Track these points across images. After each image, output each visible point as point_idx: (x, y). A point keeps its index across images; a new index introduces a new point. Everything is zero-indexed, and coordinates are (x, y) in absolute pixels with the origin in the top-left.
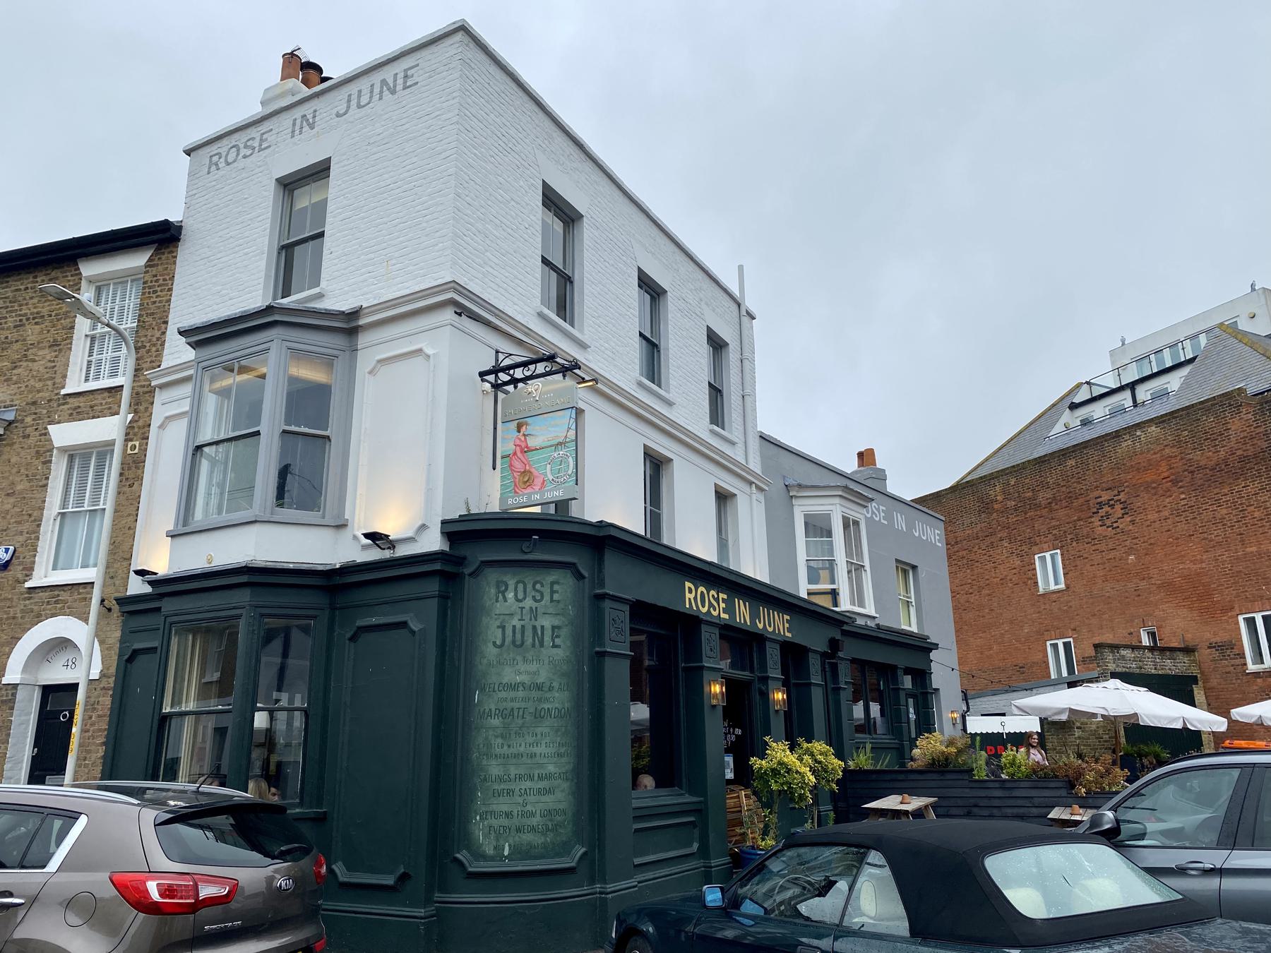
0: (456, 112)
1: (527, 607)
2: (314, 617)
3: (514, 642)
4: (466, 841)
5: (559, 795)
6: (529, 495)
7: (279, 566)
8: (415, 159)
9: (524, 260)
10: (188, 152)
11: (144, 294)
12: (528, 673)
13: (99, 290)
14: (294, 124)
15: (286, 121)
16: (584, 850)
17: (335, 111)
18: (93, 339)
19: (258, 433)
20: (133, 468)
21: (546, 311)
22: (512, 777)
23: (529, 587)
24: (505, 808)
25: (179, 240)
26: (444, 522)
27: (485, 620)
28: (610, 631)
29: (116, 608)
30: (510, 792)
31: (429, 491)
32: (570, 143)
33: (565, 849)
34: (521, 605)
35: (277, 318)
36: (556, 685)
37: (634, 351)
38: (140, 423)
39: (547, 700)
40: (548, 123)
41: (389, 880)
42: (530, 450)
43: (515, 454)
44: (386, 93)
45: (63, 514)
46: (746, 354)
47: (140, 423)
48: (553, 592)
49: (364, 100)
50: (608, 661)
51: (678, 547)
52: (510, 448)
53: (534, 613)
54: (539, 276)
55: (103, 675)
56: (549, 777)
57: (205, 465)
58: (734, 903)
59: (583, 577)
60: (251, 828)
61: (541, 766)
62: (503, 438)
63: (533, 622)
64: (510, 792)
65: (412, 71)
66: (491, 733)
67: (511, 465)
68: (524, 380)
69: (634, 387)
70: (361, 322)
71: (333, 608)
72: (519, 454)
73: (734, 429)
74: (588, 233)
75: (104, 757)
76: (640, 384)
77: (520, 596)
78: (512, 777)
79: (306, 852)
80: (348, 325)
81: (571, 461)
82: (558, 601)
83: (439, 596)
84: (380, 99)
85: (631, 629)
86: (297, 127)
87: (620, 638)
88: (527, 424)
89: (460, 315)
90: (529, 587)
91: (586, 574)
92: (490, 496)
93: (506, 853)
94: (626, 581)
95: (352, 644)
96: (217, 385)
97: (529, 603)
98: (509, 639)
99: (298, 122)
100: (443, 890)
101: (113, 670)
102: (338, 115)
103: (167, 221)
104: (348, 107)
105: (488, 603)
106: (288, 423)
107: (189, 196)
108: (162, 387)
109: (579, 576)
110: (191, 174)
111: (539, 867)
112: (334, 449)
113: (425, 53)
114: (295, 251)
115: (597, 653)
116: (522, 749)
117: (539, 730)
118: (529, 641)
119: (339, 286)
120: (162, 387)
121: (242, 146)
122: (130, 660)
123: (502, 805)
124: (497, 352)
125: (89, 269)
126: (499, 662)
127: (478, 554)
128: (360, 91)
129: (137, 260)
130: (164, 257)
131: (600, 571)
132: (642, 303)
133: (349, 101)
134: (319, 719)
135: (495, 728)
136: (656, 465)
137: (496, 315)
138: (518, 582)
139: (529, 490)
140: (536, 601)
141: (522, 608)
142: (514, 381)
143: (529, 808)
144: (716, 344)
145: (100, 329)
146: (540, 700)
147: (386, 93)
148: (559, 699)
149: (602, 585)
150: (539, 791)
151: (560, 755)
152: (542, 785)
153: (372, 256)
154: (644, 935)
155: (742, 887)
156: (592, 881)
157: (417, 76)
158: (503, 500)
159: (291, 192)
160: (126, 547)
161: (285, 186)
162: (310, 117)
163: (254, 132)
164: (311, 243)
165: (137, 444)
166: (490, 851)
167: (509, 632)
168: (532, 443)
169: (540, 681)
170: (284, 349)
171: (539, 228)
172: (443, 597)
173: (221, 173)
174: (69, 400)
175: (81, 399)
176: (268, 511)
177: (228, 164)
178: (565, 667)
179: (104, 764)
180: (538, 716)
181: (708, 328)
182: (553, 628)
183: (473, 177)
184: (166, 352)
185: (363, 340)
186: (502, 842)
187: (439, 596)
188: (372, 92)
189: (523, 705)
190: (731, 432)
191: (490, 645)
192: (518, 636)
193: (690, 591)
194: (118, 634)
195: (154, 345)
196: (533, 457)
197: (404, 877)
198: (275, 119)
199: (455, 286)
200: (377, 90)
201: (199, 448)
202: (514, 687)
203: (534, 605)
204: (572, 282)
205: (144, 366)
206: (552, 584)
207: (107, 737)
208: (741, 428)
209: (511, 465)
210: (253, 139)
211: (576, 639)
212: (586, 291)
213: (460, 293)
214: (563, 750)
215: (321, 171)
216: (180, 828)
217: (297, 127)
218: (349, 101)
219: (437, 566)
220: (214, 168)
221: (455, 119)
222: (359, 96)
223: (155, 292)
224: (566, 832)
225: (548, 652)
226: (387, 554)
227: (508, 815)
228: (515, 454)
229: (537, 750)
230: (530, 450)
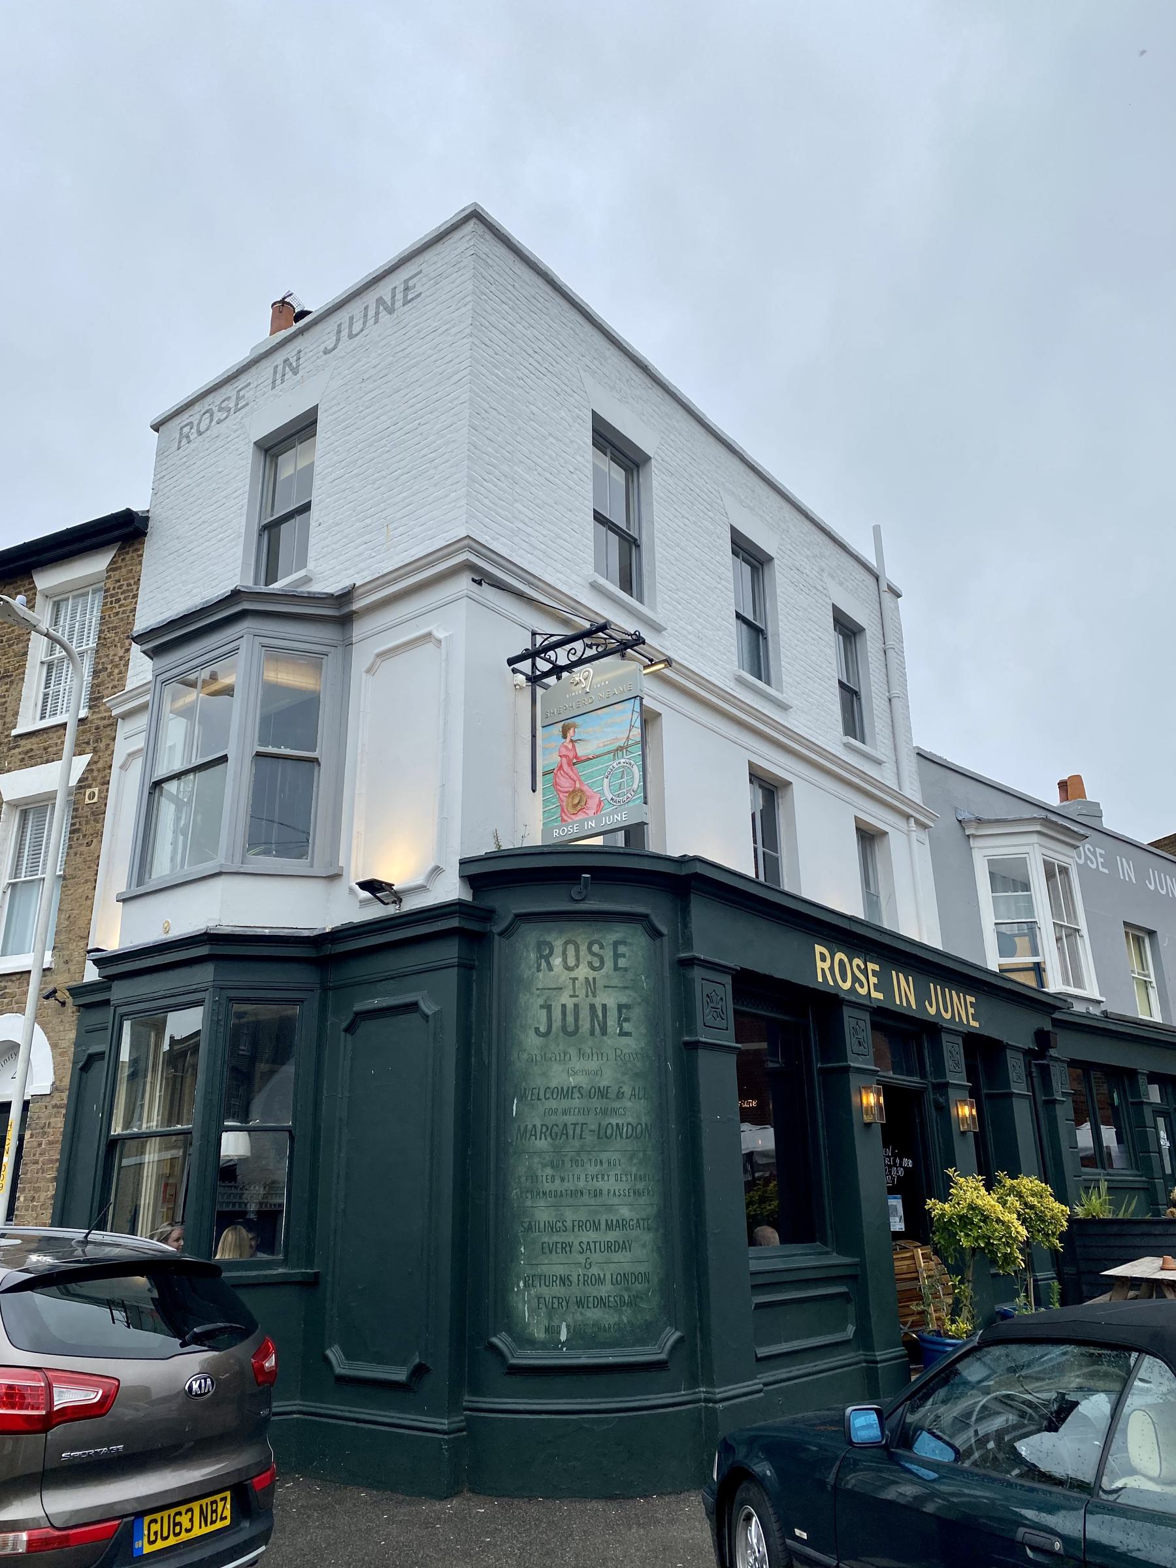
0: (470, 321)
1: (581, 978)
2: (301, 1001)
3: (564, 1028)
4: (507, 1319)
5: (639, 1252)
6: (581, 823)
7: (249, 932)
8: (419, 390)
9: (569, 515)
10: (156, 428)
11: (105, 604)
12: (588, 1073)
13: (57, 606)
14: (275, 372)
15: (265, 370)
16: (678, 1334)
17: (322, 348)
18: (50, 666)
19: (224, 759)
20: (86, 821)
21: (602, 581)
22: (569, 1224)
23: (583, 949)
24: (560, 1270)
25: (145, 534)
26: (463, 863)
27: (523, 998)
28: (703, 1013)
29: (70, 1001)
30: (566, 1247)
31: (443, 821)
32: (630, 364)
33: (646, 1333)
34: (573, 974)
35: (246, 606)
36: (627, 1089)
37: (731, 636)
38: (100, 765)
39: (615, 1111)
40: (598, 338)
41: (400, 1375)
42: (580, 761)
43: (561, 768)
44: (383, 313)
45: (14, 885)
46: (890, 642)
47: (100, 765)
48: (616, 956)
49: (357, 328)
50: (703, 1056)
51: (806, 895)
52: (554, 760)
53: (591, 986)
54: (591, 536)
55: (55, 1088)
56: (622, 1224)
57: (167, 811)
58: (904, 1438)
59: (660, 934)
60: (180, 1298)
61: (610, 1208)
62: (544, 748)
63: (590, 1000)
64: (566, 1247)
65: (415, 280)
66: (536, 1159)
67: (556, 784)
68: (569, 668)
69: (732, 684)
70: (355, 606)
71: (325, 989)
72: (565, 767)
73: (879, 742)
74: (658, 481)
75: (54, 1197)
76: (740, 681)
77: (571, 962)
78: (569, 1224)
79: (244, 1334)
80: (339, 612)
81: (637, 772)
82: (626, 969)
83: (459, 965)
84: (376, 322)
85: (736, 1012)
86: (279, 376)
87: (718, 1023)
88: (575, 726)
89: (480, 583)
90: (583, 949)
91: (664, 929)
92: (529, 826)
93: (563, 1337)
94: (719, 937)
95: (349, 1036)
96: (180, 703)
97: (583, 972)
98: (557, 1024)
99: (280, 368)
100: (476, 1391)
101: (66, 1082)
102: (326, 352)
103: (128, 509)
104: (338, 340)
105: (527, 974)
106: (263, 741)
107: (158, 479)
108: (125, 716)
109: (655, 933)
110: (161, 453)
111: (611, 1360)
112: (324, 776)
113: (429, 255)
114: (274, 532)
115: (686, 1044)
116: (582, 1184)
117: (604, 1156)
118: (585, 1026)
119: (327, 563)
120: (125, 716)
121: (215, 409)
122: (85, 1068)
123: (555, 1266)
124: (534, 634)
125: (46, 580)
126: (544, 1057)
127: (511, 904)
128: (351, 318)
129: (96, 565)
130: (128, 557)
131: (685, 925)
132: (738, 577)
133: (339, 332)
134: (307, 1143)
135: (540, 1153)
136: (769, 789)
137: (529, 584)
138: (566, 943)
139: (581, 816)
140: (594, 969)
141: (574, 979)
142: (557, 670)
143: (595, 1270)
144: (847, 630)
145: (59, 653)
146: (604, 1112)
147: (383, 313)
148: (633, 1111)
149: (688, 944)
150: (610, 1247)
151: (637, 1193)
152: (611, 1236)
153: (368, 521)
154: (758, 1480)
155: (913, 1410)
156: (693, 1382)
157: (419, 286)
158: (546, 831)
159: (276, 457)
160: (81, 923)
161: (266, 451)
162: (293, 360)
163: (229, 391)
164: (298, 518)
165: (96, 790)
166: (540, 1334)
167: (557, 1013)
168: (582, 750)
169: (604, 1083)
170: (257, 646)
171: (589, 473)
172: (466, 967)
173: (193, 446)
174: (22, 742)
175: (34, 740)
176: (238, 857)
177: (200, 433)
178: (639, 1064)
179: (54, 1206)
180: (603, 1135)
181: (835, 607)
182: (620, 1007)
183: (494, 404)
184: (130, 673)
185: (359, 630)
186: (555, 1323)
187: (459, 965)
188: (366, 316)
189: (581, 1119)
190: (875, 747)
191: (532, 1033)
192: (570, 1019)
193: (823, 959)
194: (72, 1035)
195: (117, 666)
196: (583, 770)
197: (420, 1371)
198: (253, 370)
199: (469, 543)
200: (371, 313)
201: (157, 785)
202: (565, 1093)
203: (592, 975)
204: (638, 546)
205: (106, 692)
206: (616, 944)
207: (58, 1170)
208: (889, 743)
209: (556, 784)
210: (228, 398)
211: (654, 1025)
212: (658, 556)
213: (478, 554)
214: (640, 1186)
215: (303, 428)
216: (37, 1298)
217: (279, 376)
218: (339, 332)
219: (454, 923)
220: (184, 441)
221: (468, 331)
222: (351, 325)
223: (118, 600)
224: (650, 1306)
225: (612, 1042)
226: (392, 910)
227: (564, 1281)
228: (561, 768)
229: (600, 1184)
230: (580, 761)
